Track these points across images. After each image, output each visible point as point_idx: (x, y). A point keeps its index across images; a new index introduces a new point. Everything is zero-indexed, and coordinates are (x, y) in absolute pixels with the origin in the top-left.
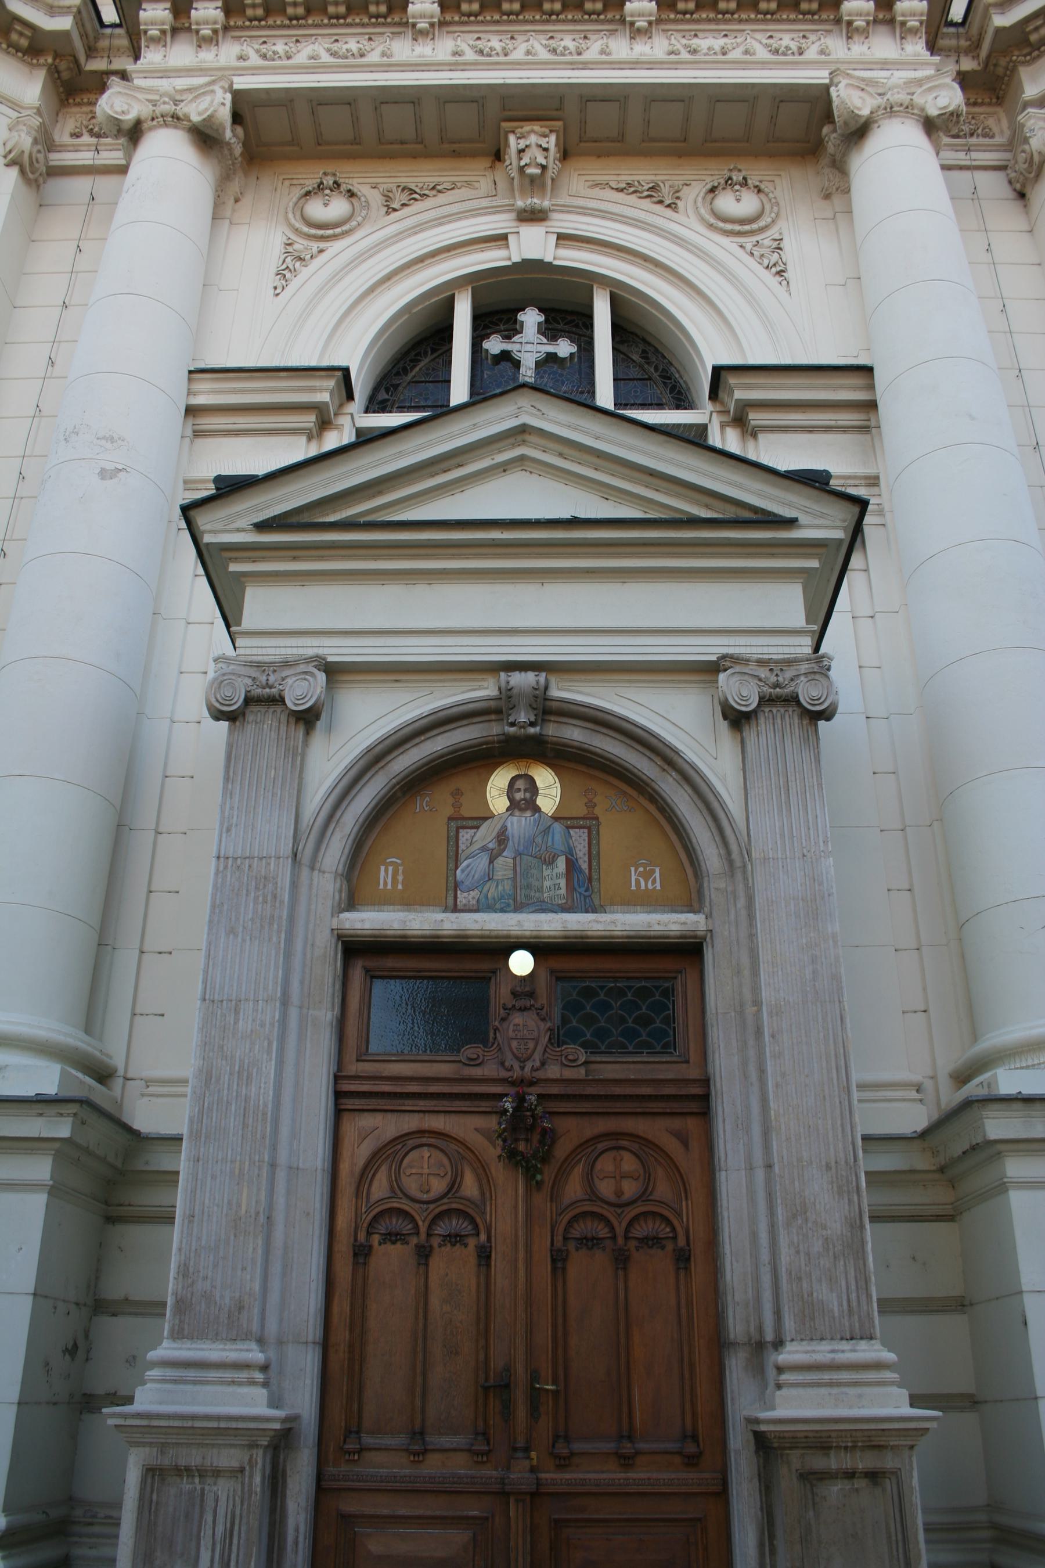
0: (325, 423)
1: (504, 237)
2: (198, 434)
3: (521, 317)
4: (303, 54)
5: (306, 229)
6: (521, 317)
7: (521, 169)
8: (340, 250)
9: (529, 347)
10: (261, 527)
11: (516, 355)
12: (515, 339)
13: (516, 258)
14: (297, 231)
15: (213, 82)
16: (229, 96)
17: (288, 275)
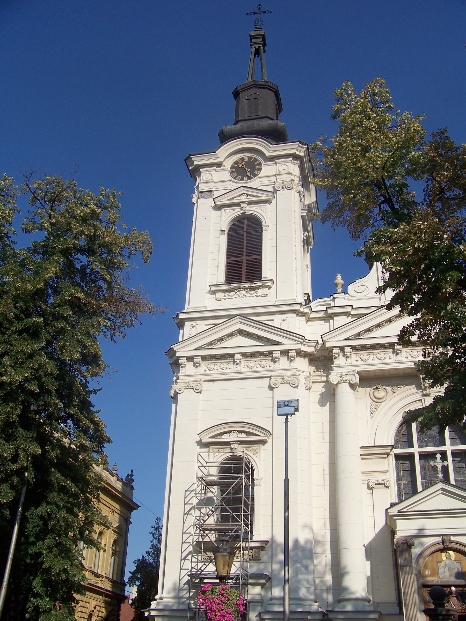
0: (388, 454)
1: (421, 400)
2: (362, 459)
3: (436, 456)
4: (371, 357)
5: (376, 400)
6: (436, 456)
7: (424, 385)
8: (384, 407)
9: (439, 464)
10: (399, 511)
11: (437, 466)
12: (436, 461)
13: (424, 406)
14: (373, 401)
15: (354, 371)
16: (357, 375)
17: (374, 414)
